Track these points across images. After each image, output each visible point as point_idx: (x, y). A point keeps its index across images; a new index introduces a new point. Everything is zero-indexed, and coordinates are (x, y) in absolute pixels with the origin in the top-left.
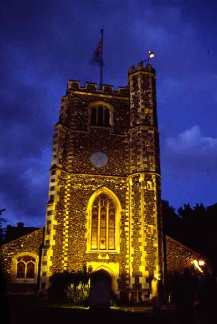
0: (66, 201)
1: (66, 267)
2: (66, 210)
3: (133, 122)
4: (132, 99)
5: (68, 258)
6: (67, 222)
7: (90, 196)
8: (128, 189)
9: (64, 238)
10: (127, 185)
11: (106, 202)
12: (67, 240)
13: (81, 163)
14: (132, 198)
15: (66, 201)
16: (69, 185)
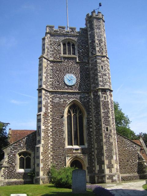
1: (52, 159)
2: (49, 118)
3: (91, 53)
4: (89, 36)
5: (53, 153)
6: (51, 127)
8: (90, 100)
9: (50, 138)
10: (90, 97)
11: (76, 110)
12: (51, 140)
13: (58, 83)
14: (94, 107)
15: (49, 111)
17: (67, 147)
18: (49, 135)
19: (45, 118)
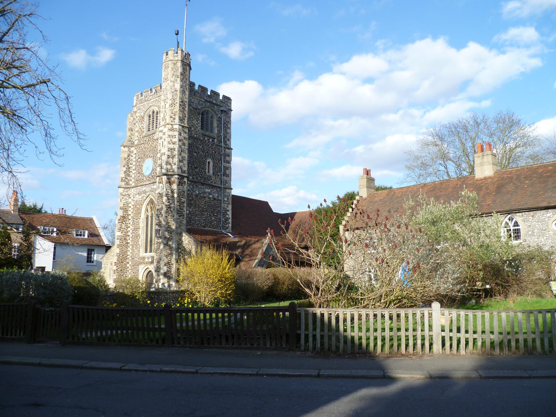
0: (130, 213)
6: (131, 231)
7: (142, 205)
12: (131, 247)
16: (132, 198)
17: (142, 254)
18: (129, 241)
19: (122, 222)
